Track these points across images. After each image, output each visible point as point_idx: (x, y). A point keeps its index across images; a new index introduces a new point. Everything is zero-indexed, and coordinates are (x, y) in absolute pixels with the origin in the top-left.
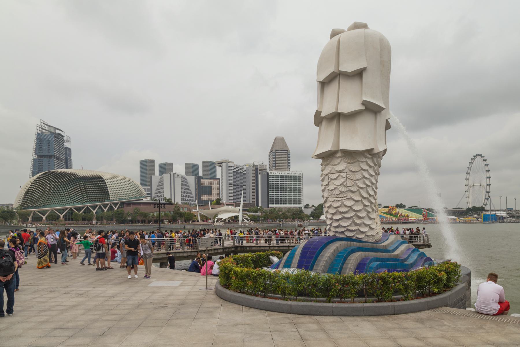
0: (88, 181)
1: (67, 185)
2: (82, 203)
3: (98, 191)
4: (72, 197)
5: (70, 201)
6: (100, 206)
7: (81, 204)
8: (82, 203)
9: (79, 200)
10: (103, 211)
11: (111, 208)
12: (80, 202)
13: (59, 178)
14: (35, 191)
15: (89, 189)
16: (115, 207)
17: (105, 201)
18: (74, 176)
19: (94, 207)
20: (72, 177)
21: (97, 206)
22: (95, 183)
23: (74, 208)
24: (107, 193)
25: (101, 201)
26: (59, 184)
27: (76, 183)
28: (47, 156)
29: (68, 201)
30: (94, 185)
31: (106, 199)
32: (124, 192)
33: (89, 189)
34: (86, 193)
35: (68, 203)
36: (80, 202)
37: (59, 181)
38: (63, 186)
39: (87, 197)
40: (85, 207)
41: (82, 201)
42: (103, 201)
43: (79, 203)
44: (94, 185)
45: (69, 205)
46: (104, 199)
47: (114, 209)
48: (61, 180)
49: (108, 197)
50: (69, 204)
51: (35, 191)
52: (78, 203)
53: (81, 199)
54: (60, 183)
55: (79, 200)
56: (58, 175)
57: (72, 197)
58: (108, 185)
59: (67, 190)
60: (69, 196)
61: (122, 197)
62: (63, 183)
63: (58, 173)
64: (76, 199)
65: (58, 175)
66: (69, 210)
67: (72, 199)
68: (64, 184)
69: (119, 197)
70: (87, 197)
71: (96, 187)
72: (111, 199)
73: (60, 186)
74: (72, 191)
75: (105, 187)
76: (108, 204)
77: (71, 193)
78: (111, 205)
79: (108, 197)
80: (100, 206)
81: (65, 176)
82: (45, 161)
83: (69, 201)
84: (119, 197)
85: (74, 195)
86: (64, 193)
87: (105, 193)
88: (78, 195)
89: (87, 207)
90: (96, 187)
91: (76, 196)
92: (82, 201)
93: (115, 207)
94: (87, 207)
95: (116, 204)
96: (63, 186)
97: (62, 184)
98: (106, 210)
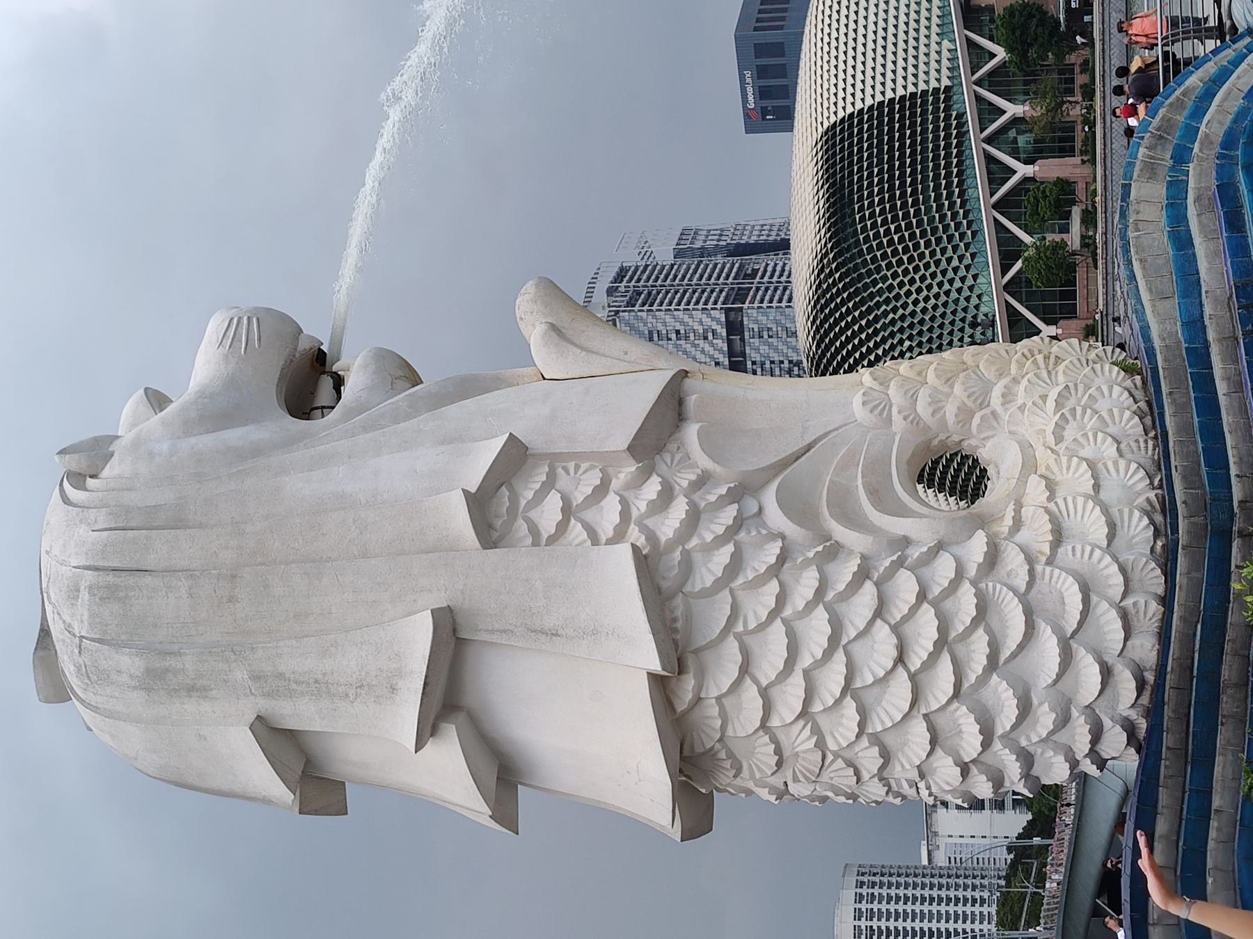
0: (851, 202)
1: (878, 305)
2: (974, 234)
3: (902, 165)
4: (940, 285)
5: (966, 293)
6: (989, 140)
7: (979, 236)
8: (974, 234)
9: (955, 248)
10: (1016, 121)
12: (967, 246)
13: (843, 345)
15: (892, 197)
16: (993, 56)
17: (960, 116)
18: (831, 274)
19: (997, 173)
20: (834, 284)
21: (989, 159)
22: (860, 170)
23: (1004, 273)
25: (962, 135)
26: (877, 346)
27: (865, 263)
28: (730, 343)
29: (957, 284)
30: (870, 175)
31: (948, 109)
32: (902, 18)
33: (892, 197)
34: (917, 213)
35: (974, 301)
36: (967, 246)
37: (861, 343)
38: (884, 327)
39: (940, 207)
40: (995, 219)
41: (962, 236)
42: (961, 124)
43: (972, 250)
44: (870, 175)
45: (985, 298)
46: (947, 118)
47: (1004, 64)
48: (854, 335)
49: (936, 100)
50: (979, 297)
52: (973, 256)
53: (950, 238)
54: (869, 338)
55: (955, 248)
56: (827, 348)
57: (940, 285)
58: (869, 102)
59: (905, 306)
60: (937, 296)
61: (935, 20)
62: (869, 324)
63: (818, 346)
64: (955, 263)
65: (827, 348)
67: (951, 282)
68: (876, 319)
69: (934, 38)
70: (940, 207)
71: (880, 162)
72: (945, 82)
73: (884, 340)
74: (911, 260)
75: (881, 114)
76: (979, 99)
77: (916, 269)
78: (978, 83)
79: (936, 100)
80: (989, 140)
81: (832, 313)
82: (755, 350)
83: (963, 279)
84: (934, 38)
85: (933, 276)
86: (913, 314)
87: (913, 115)
88: (933, 254)
89: (995, 206)
90: (880, 162)
91: (937, 263)
92: (962, 236)
93: (993, 56)
94: (995, 206)
95: (977, 55)
96: (884, 327)
97: (876, 332)
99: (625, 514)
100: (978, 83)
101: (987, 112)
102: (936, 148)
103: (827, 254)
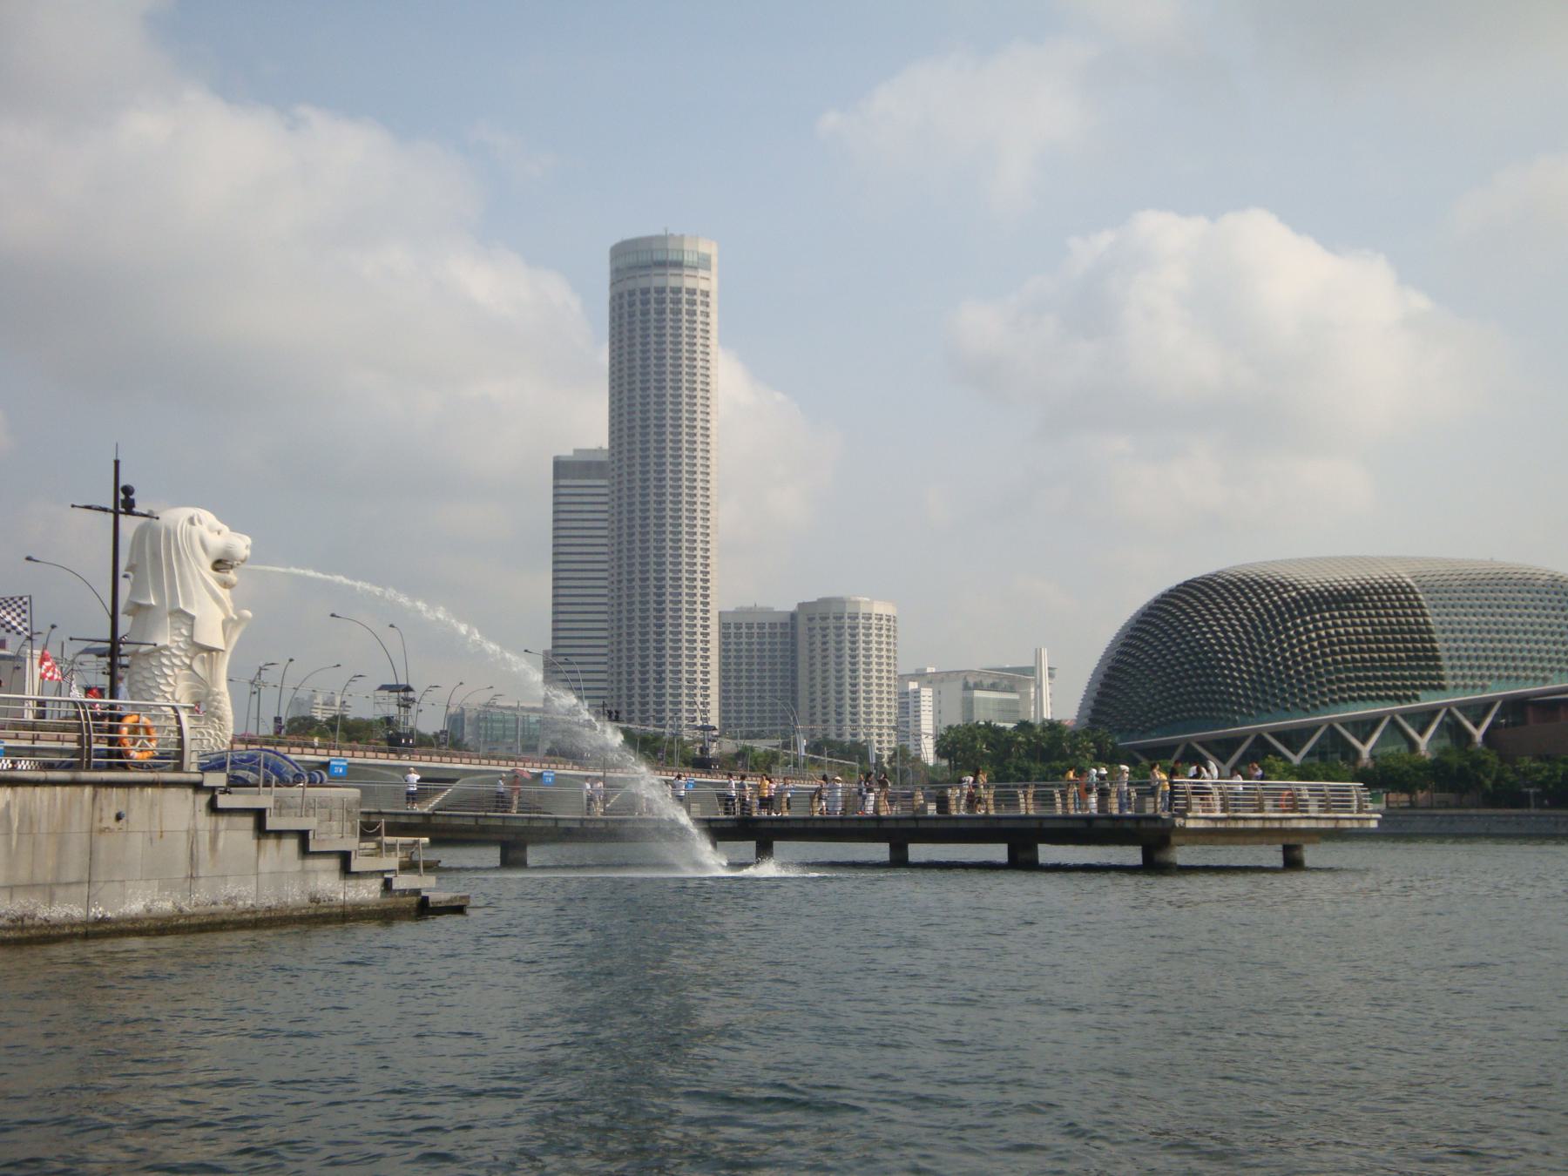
6: (1393, 722)
10: (1413, 745)
11: (1454, 730)
14: (1132, 665)
17: (1417, 698)
19: (1364, 727)
24: (1428, 658)
25: (1398, 699)
31: (1423, 687)
37: (1217, 620)
40: (1319, 727)
42: (1408, 699)
46: (1414, 687)
51: (1132, 665)
66: (1255, 741)
76: (1433, 712)
80: (1393, 722)
94: (1331, 728)
98: (1423, 742)
99: (177, 642)
100: (1449, 713)
101: (1423, 719)
102: (1376, 678)
103: (1295, 588)
